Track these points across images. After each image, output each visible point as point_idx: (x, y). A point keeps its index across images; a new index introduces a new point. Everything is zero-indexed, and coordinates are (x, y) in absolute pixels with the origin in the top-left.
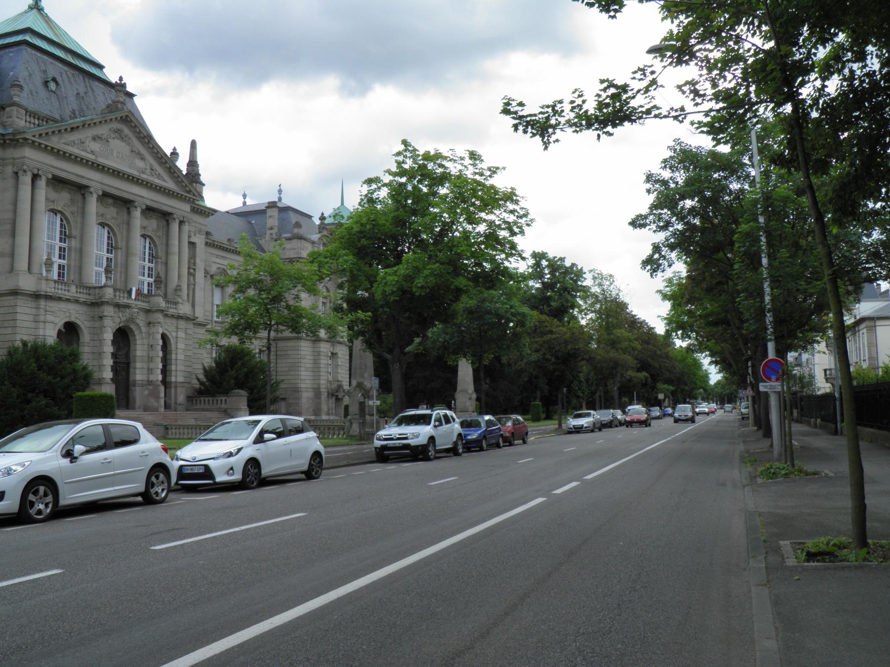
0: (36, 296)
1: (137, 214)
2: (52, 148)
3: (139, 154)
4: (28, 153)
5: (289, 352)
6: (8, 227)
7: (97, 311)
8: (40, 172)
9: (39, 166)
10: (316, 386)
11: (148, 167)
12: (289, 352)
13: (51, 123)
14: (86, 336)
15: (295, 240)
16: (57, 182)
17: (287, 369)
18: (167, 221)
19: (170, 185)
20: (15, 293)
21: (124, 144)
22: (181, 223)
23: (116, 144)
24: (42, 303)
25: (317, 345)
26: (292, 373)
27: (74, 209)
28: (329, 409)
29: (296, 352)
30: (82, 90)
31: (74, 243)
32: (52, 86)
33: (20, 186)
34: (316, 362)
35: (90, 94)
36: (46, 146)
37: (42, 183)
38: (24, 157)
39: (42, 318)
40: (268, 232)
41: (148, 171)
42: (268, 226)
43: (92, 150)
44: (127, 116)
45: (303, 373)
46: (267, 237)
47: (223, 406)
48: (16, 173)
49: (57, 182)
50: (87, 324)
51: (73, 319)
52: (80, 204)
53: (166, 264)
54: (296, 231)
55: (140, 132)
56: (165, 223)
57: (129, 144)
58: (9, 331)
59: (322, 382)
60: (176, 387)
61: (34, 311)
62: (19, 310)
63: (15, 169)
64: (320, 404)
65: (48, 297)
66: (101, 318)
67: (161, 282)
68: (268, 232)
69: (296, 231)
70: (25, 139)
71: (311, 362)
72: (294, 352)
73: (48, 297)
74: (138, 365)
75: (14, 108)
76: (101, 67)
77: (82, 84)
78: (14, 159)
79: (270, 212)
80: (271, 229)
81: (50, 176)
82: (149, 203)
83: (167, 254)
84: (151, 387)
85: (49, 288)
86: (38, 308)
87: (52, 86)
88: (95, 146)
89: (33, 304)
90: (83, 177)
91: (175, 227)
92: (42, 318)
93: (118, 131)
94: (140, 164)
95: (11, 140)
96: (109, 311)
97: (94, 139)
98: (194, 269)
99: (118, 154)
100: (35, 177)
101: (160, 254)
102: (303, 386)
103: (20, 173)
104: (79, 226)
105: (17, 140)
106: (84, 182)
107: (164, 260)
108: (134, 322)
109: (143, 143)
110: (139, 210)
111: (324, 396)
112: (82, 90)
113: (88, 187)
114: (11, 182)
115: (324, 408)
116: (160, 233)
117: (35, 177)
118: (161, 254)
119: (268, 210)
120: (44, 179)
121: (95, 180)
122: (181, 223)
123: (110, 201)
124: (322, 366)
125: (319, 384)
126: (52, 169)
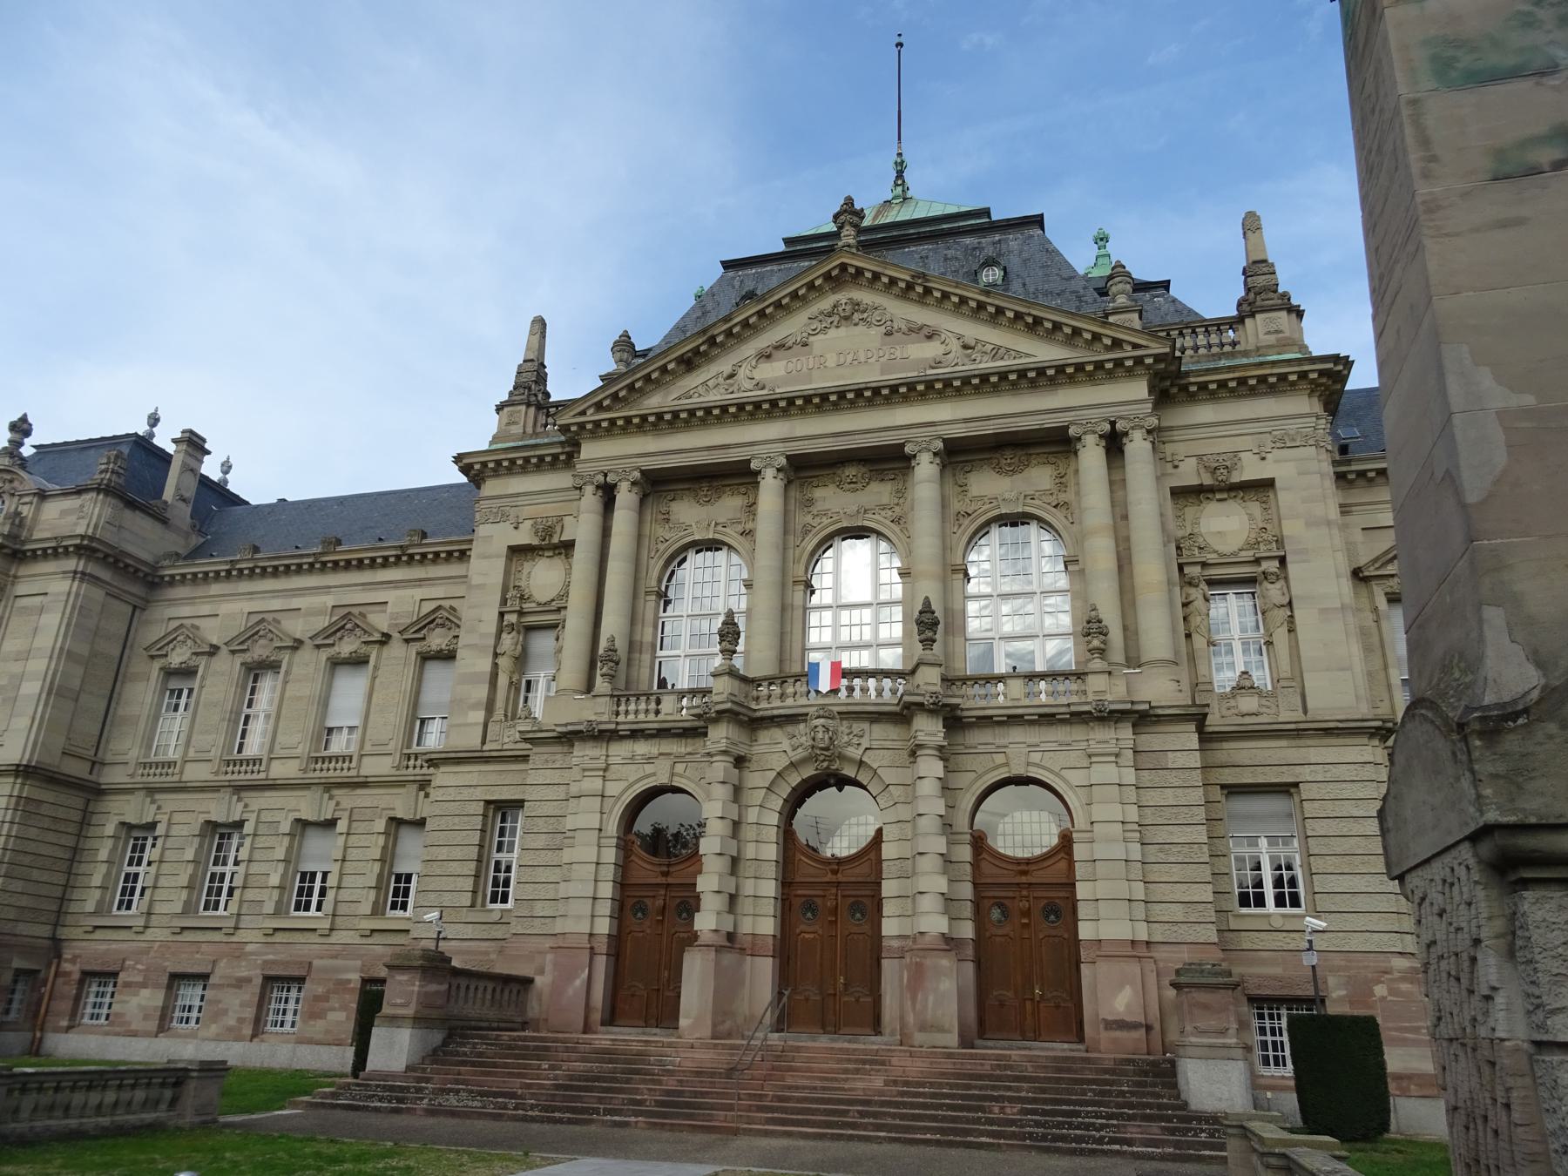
0: (569, 738)
2: (644, 418)
8: (611, 479)
9: (605, 466)
11: (955, 346)
21: (861, 328)
22: (1114, 443)
37: (625, 497)
76: (986, 212)
82: (958, 431)
92: (574, 789)
94: (931, 350)
97: (765, 356)
98: (1282, 560)
100: (608, 493)
108: (842, 757)
117: (608, 493)
121: (764, 441)
123: (851, 471)
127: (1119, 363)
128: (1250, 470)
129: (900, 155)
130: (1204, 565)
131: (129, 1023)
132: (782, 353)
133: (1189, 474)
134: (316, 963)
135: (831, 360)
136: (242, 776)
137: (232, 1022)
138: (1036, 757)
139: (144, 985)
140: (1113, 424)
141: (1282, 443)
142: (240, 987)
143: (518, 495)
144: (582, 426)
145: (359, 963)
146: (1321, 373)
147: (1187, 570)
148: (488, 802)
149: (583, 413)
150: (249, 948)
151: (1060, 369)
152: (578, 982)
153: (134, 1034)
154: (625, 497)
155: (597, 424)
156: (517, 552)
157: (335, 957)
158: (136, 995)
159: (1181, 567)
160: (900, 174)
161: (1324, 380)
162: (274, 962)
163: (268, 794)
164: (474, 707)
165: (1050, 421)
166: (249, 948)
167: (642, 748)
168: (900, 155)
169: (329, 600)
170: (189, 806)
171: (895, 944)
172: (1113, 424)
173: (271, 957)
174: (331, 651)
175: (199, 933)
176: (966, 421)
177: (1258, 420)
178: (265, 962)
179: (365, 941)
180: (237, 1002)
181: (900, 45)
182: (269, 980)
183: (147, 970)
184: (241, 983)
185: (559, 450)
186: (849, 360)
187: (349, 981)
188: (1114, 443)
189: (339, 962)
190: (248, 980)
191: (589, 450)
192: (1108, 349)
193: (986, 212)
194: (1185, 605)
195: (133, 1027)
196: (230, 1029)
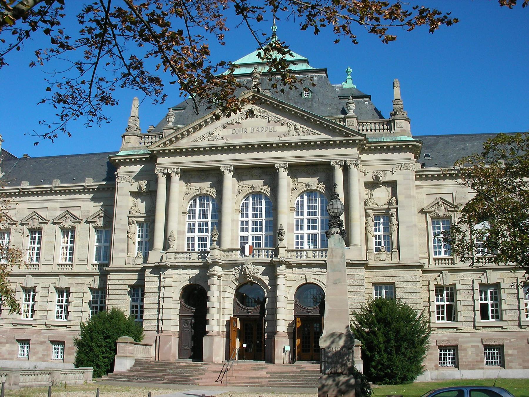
36: (175, 150)
37: (176, 178)
82: (294, 161)
94: (285, 129)
98: (397, 209)
100: (169, 177)
117: (169, 177)
127: (347, 141)
128: (389, 178)
130: (373, 209)
131: (3, 356)
132: (231, 126)
133: (369, 178)
134: (68, 336)
135: (249, 131)
137: (41, 356)
138: (315, 277)
139: (7, 343)
140: (345, 162)
141: (401, 168)
144: (158, 151)
146: (413, 145)
147: (367, 211)
148: (128, 285)
149: (159, 146)
150: (43, 331)
151: (328, 142)
152: (168, 346)
153: (6, 359)
154: (176, 178)
155: (164, 151)
158: (5, 346)
159: (366, 210)
161: (413, 148)
162: (52, 336)
164: (122, 251)
165: (325, 159)
166: (43, 331)
172: (345, 162)
174: (61, 225)
176: (296, 157)
177: (393, 160)
180: (41, 349)
184: (42, 343)
186: (255, 130)
188: (346, 169)
190: (44, 342)
191: (160, 160)
192: (344, 136)
194: (366, 223)
195: (5, 357)
196: (40, 358)
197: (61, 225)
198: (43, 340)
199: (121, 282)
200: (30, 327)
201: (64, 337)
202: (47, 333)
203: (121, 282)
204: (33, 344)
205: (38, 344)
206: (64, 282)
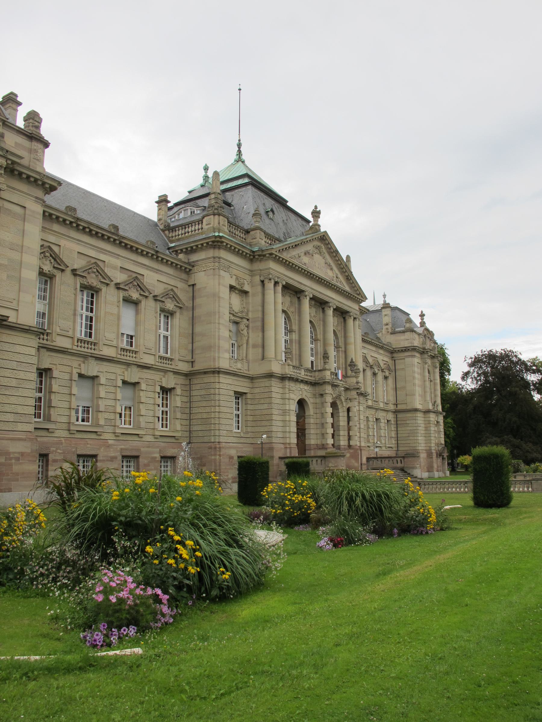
0: (283, 378)
1: (330, 312)
3: (329, 265)
4: (272, 265)
5: (408, 422)
6: (259, 324)
7: (318, 389)
10: (428, 448)
12: (408, 422)
13: (277, 242)
14: (311, 410)
15: (408, 333)
16: (287, 288)
17: (407, 435)
18: (344, 318)
19: (347, 288)
20: (270, 376)
21: (321, 258)
23: (317, 257)
24: (287, 383)
25: (428, 415)
26: (411, 438)
27: (292, 309)
28: (438, 467)
29: (414, 421)
30: (285, 218)
31: (295, 336)
32: (271, 214)
33: (266, 292)
34: (427, 429)
35: (289, 220)
38: (270, 268)
39: (287, 396)
40: (384, 327)
41: (335, 278)
42: (385, 322)
43: (305, 261)
44: (324, 235)
45: (420, 438)
46: (384, 331)
47: (399, 465)
48: (263, 282)
49: (287, 288)
50: (312, 400)
51: (304, 397)
52: (297, 306)
53: (345, 352)
54: (408, 325)
55: (331, 248)
56: (342, 320)
57: (324, 258)
58: (266, 406)
59: (433, 445)
60: (361, 450)
61: (281, 391)
62: (273, 389)
63: (262, 278)
64: (432, 462)
65: (291, 379)
66: (322, 395)
67: (350, 365)
68: (384, 327)
69: (408, 325)
70: (271, 254)
71: (424, 429)
72: (412, 422)
73: (291, 379)
74: (342, 433)
75: (258, 231)
76: (287, 202)
77: (284, 213)
78: (261, 270)
79: (385, 312)
80: (387, 324)
81: (284, 283)
83: (346, 344)
84: (351, 451)
85: (289, 371)
86: (283, 388)
87: (271, 214)
88: (305, 259)
89: (280, 385)
90: (301, 283)
91: (350, 322)
93: (318, 248)
94: (330, 273)
95: (259, 256)
96: (328, 389)
99: (318, 265)
101: (340, 344)
102: (420, 448)
103: (266, 281)
104: (297, 322)
105: (264, 256)
106: (302, 288)
107: (343, 349)
109: (331, 257)
110: (332, 309)
111: (434, 455)
112: (285, 218)
113: (303, 291)
114: (259, 288)
115: (435, 466)
116: (339, 328)
118: (341, 344)
119: (383, 310)
120: (280, 284)
122: (355, 318)
124: (432, 432)
125: (430, 447)
126: (285, 278)
129: (239, 140)
134: (142, 449)
136: (82, 349)
142: (112, 461)
143: (232, 263)
145: (158, 450)
148: (235, 391)
156: (232, 288)
157: (149, 447)
160: (239, 148)
162: (126, 449)
163: (105, 363)
166: (110, 442)
167: (302, 386)
168: (239, 140)
169: (118, 263)
170: (65, 362)
171: (343, 447)
173: (123, 447)
175: (83, 433)
176: (339, 302)
178: (122, 449)
179: (156, 440)
181: (240, 90)
182: (124, 457)
183: (64, 453)
184: (112, 459)
185: (249, 252)
187: (156, 458)
189: (150, 449)
190: (116, 458)
193: (287, 202)
197: (126, 294)
198: (113, 455)
199: (229, 387)
200: (93, 436)
201: (139, 450)
202: (117, 445)
203: (229, 387)
204: (103, 461)
205: (107, 460)
206: (133, 375)
